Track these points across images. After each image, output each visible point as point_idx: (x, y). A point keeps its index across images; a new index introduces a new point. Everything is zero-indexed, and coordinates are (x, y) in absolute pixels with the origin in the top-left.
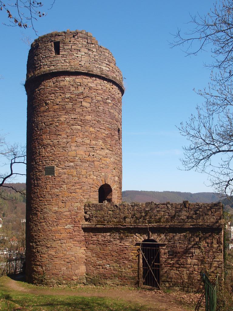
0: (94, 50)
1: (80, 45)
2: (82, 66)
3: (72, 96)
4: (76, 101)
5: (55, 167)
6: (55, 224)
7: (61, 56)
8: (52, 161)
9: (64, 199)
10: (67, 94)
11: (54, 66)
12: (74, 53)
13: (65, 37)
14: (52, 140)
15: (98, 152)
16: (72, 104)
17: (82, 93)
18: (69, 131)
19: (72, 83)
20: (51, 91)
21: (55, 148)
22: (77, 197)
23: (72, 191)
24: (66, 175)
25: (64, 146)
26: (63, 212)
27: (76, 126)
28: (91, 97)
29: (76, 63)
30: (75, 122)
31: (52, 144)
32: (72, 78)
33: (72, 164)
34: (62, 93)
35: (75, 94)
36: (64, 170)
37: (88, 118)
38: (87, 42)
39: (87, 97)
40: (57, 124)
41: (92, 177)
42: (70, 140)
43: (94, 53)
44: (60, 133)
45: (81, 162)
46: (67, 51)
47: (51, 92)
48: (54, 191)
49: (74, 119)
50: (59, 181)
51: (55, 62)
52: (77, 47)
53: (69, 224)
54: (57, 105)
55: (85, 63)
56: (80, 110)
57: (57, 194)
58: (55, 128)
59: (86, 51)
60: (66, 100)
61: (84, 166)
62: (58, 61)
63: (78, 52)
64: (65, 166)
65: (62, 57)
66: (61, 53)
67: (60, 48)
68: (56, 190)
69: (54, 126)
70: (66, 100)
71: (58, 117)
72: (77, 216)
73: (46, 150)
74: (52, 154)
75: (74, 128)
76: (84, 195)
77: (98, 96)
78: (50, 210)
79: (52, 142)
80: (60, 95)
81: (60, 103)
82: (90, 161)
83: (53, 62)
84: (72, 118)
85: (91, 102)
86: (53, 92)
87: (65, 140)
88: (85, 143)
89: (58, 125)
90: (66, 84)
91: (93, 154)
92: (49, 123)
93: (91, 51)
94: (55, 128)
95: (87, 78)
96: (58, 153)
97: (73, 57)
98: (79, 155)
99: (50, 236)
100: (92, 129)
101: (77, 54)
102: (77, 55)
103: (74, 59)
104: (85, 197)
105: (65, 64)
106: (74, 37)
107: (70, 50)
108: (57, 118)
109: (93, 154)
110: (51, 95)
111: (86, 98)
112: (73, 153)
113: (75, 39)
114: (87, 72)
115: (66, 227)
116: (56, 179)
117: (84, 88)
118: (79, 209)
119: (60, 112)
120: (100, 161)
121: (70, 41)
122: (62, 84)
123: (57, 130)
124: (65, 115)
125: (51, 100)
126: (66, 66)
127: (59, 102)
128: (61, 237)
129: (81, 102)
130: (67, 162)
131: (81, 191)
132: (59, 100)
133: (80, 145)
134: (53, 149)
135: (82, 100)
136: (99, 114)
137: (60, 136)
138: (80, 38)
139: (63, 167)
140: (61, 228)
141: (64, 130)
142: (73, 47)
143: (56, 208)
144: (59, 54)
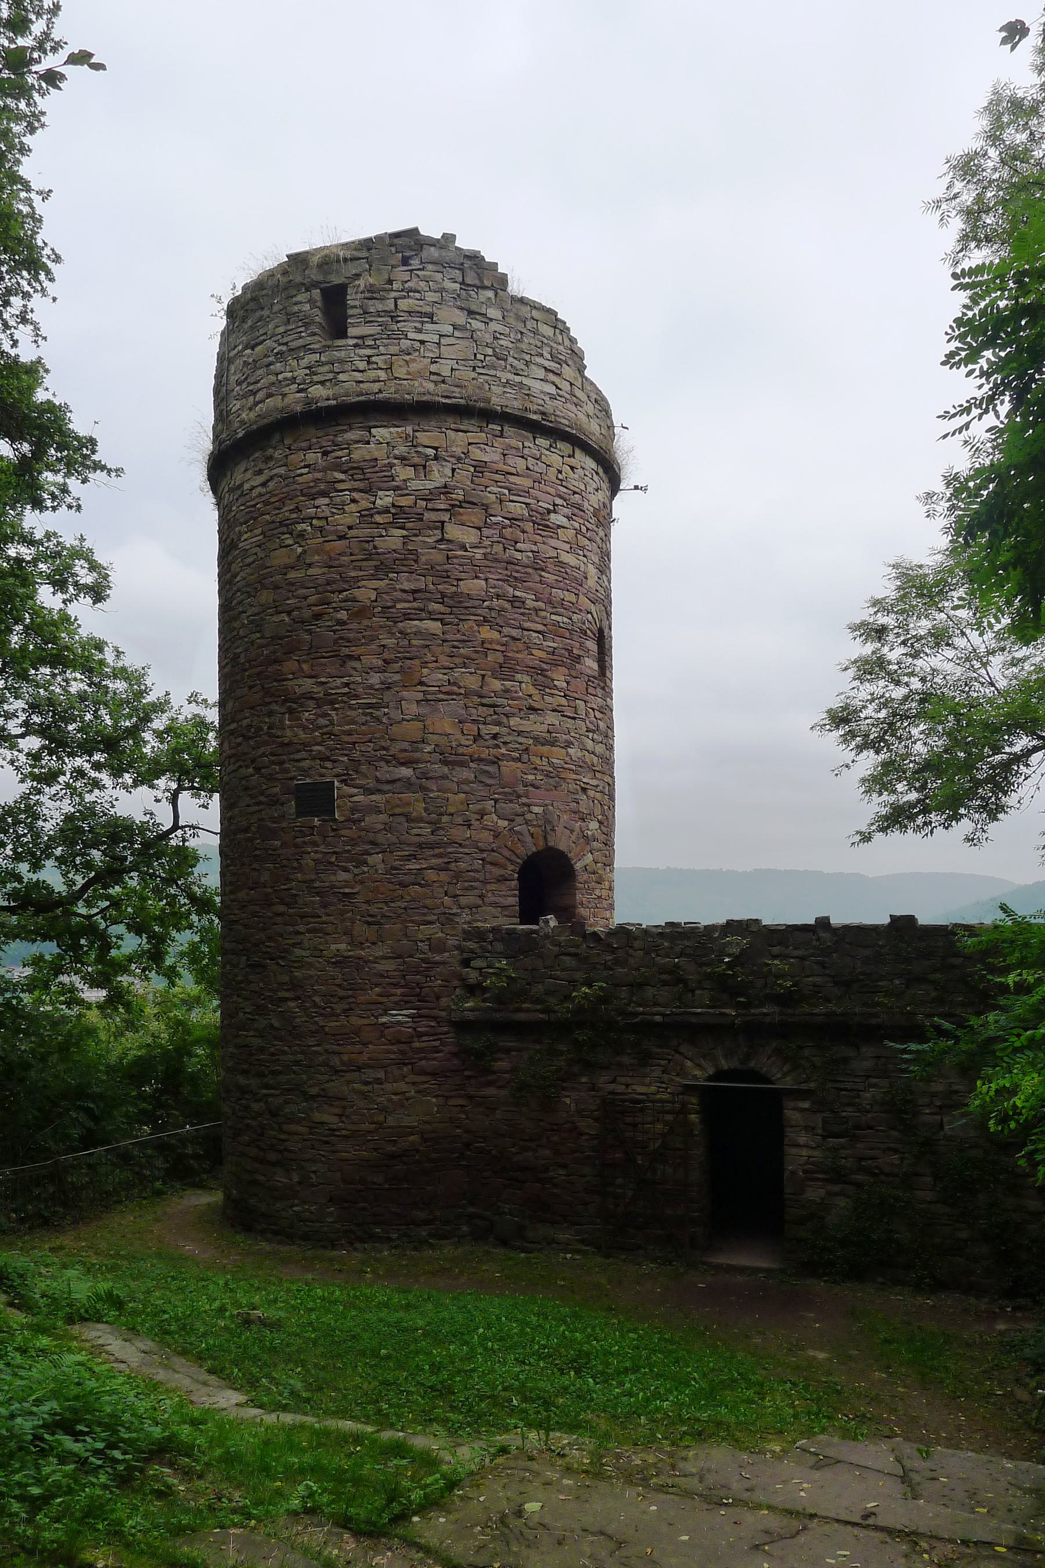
0: (493, 313)
1: (432, 297)
2: (440, 379)
3: (404, 502)
4: (421, 520)
5: (336, 784)
6: (339, 1008)
7: (351, 342)
8: (321, 759)
9: (373, 910)
10: (380, 493)
11: (322, 383)
12: (408, 327)
13: (370, 266)
14: (323, 680)
15: (514, 721)
16: (405, 533)
17: (445, 487)
18: (390, 642)
19: (401, 450)
20: (312, 484)
21: (335, 709)
22: (428, 902)
23: (407, 879)
24: (383, 817)
25: (374, 701)
26: (369, 961)
27: (421, 620)
28: (483, 505)
29: (414, 367)
30: (415, 605)
31: (321, 695)
32: (399, 430)
33: (406, 772)
34: (361, 491)
35: (417, 493)
36: (373, 797)
37: (474, 586)
38: (463, 283)
39: (464, 505)
40: (343, 615)
41: (488, 820)
42: (397, 677)
43: (494, 326)
44: (357, 651)
45: (445, 763)
46: (380, 319)
47: (314, 490)
48: (333, 878)
49: (414, 592)
50: (353, 839)
51: (326, 368)
52: (421, 303)
53: (398, 1006)
54: (341, 538)
55: (455, 366)
56: (438, 557)
57: (347, 890)
58: (334, 631)
59: (461, 318)
60: (378, 518)
61: (455, 779)
62: (342, 362)
63: (423, 323)
64: (378, 780)
65: (356, 346)
66: (352, 331)
67: (350, 312)
68: (343, 876)
69: (330, 623)
70: (378, 518)
71: (346, 586)
72: (432, 973)
73: (300, 719)
74: (323, 734)
75: (414, 630)
76: (458, 892)
77: (512, 498)
78: (317, 952)
79: (319, 689)
80: (353, 501)
81: (352, 533)
82: (480, 760)
83: (321, 369)
84: (404, 591)
85: (482, 524)
86: (322, 486)
87: (375, 679)
88: (460, 687)
89: (345, 618)
90: (376, 454)
91: (496, 729)
92: (307, 614)
93: (478, 317)
94: (334, 631)
95: (462, 427)
96: (347, 727)
97: (405, 344)
98: (435, 737)
99: (316, 1052)
100: (487, 633)
101: (420, 331)
102: (420, 337)
103: (409, 354)
104: (463, 901)
105: (372, 374)
106: (405, 261)
107: (392, 317)
108: (340, 592)
109: (496, 729)
110: (314, 499)
111: (461, 507)
112: (413, 729)
113: (411, 271)
114: (462, 402)
115: (384, 1019)
116: (342, 832)
117: (453, 470)
118: (438, 947)
119: (355, 568)
120: (525, 757)
121: (390, 282)
122: (359, 453)
123: (342, 638)
124: (374, 577)
125: (314, 522)
126: (374, 381)
127: (350, 528)
128: (365, 1057)
129: (443, 522)
130: (382, 764)
131: (444, 876)
132: (349, 520)
133: (441, 696)
134: (325, 715)
135: (446, 517)
136: (517, 571)
137: (356, 664)
138: (430, 267)
139: (371, 784)
140: (366, 1021)
141: (373, 639)
142: (403, 304)
143: (343, 946)
144: (342, 334)
